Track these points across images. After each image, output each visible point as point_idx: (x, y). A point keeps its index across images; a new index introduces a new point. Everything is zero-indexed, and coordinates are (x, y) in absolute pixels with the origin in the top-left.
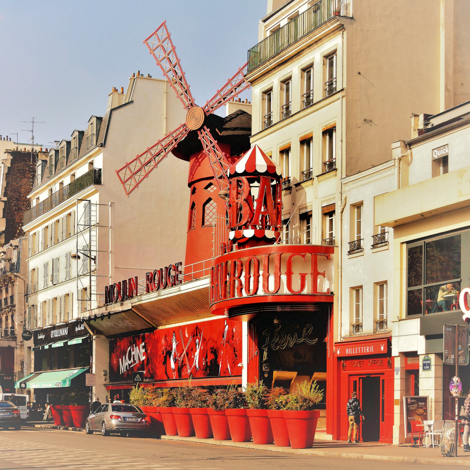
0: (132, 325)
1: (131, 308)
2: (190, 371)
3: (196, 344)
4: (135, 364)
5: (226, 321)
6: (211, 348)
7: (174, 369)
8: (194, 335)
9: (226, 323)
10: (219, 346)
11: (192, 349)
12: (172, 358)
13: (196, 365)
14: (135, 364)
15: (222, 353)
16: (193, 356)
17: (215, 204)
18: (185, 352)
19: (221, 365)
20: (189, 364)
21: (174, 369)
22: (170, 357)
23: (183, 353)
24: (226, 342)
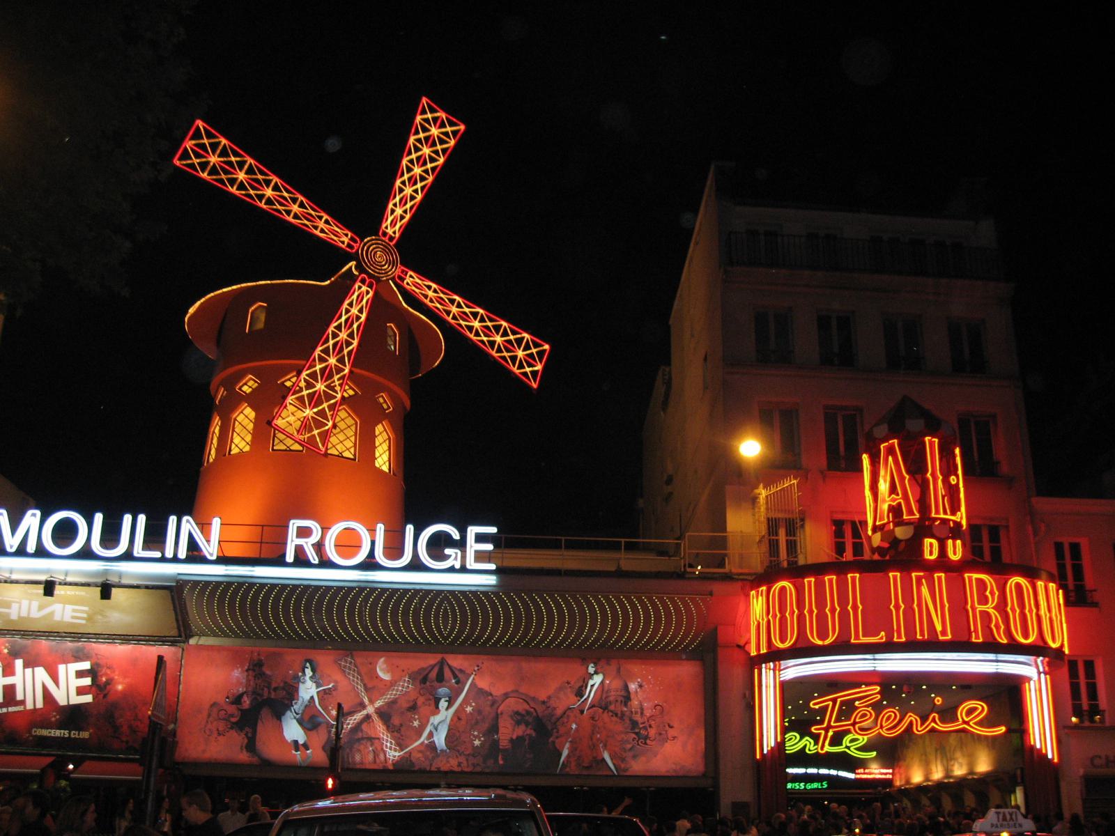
0: (73, 617)
1: (174, 584)
2: (399, 754)
3: (437, 701)
4: (11, 709)
5: (592, 665)
6: (517, 713)
7: (301, 742)
8: (427, 675)
9: (591, 670)
10: (559, 712)
11: (413, 708)
12: (289, 714)
13: (434, 742)
14: (11, 709)
15: (574, 726)
16: (416, 724)
17: (350, 421)
18: (370, 710)
19: (572, 750)
20: (393, 737)
21: (301, 742)
22: (279, 716)
23: (360, 711)
24: (592, 706)
